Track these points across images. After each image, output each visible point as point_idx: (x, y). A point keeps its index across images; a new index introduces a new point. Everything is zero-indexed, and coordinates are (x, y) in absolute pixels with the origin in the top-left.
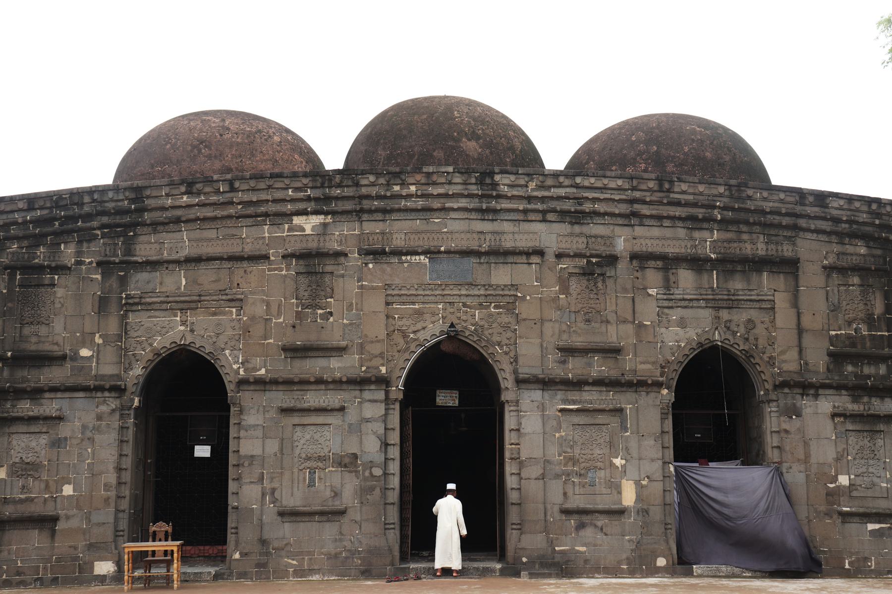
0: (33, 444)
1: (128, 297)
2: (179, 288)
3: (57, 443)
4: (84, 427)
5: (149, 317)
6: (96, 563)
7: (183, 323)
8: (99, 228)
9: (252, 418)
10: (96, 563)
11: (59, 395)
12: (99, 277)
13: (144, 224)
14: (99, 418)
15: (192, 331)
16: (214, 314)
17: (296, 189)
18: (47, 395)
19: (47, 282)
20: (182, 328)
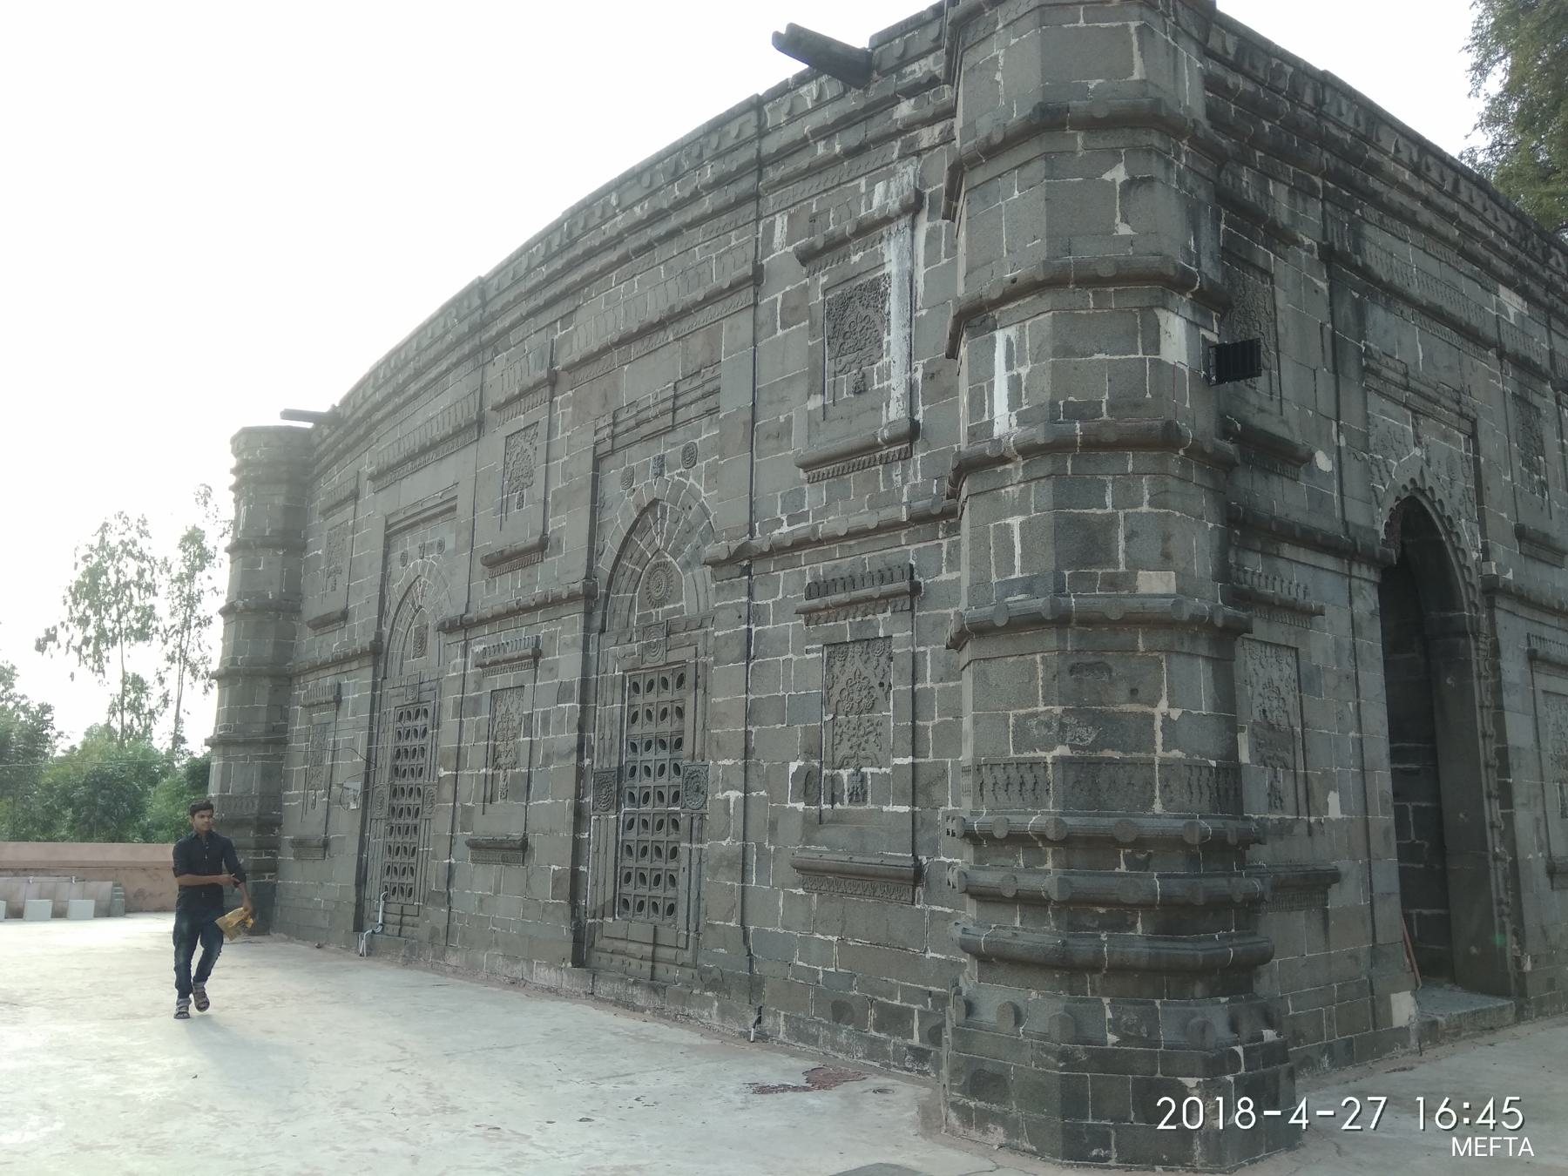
0: (1276, 676)
1: (1368, 354)
2: (1417, 363)
3: (1305, 681)
4: (1338, 644)
5: (1382, 412)
6: (1393, 996)
7: (1418, 441)
8: (1324, 177)
9: (1513, 668)
10: (1393, 996)
11: (1304, 555)
12: (1323, 285)
13: (1373, 198)
14: (1355, 627)
15: (1428, 462)
16: (1446, 437)
17: (1499, 233)
18: (1287, 550)
19: (1261, 262)
20: (1417, 451)
